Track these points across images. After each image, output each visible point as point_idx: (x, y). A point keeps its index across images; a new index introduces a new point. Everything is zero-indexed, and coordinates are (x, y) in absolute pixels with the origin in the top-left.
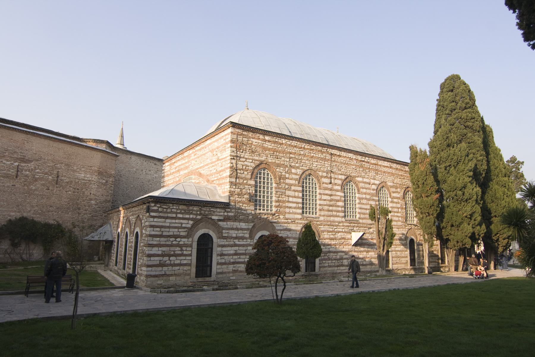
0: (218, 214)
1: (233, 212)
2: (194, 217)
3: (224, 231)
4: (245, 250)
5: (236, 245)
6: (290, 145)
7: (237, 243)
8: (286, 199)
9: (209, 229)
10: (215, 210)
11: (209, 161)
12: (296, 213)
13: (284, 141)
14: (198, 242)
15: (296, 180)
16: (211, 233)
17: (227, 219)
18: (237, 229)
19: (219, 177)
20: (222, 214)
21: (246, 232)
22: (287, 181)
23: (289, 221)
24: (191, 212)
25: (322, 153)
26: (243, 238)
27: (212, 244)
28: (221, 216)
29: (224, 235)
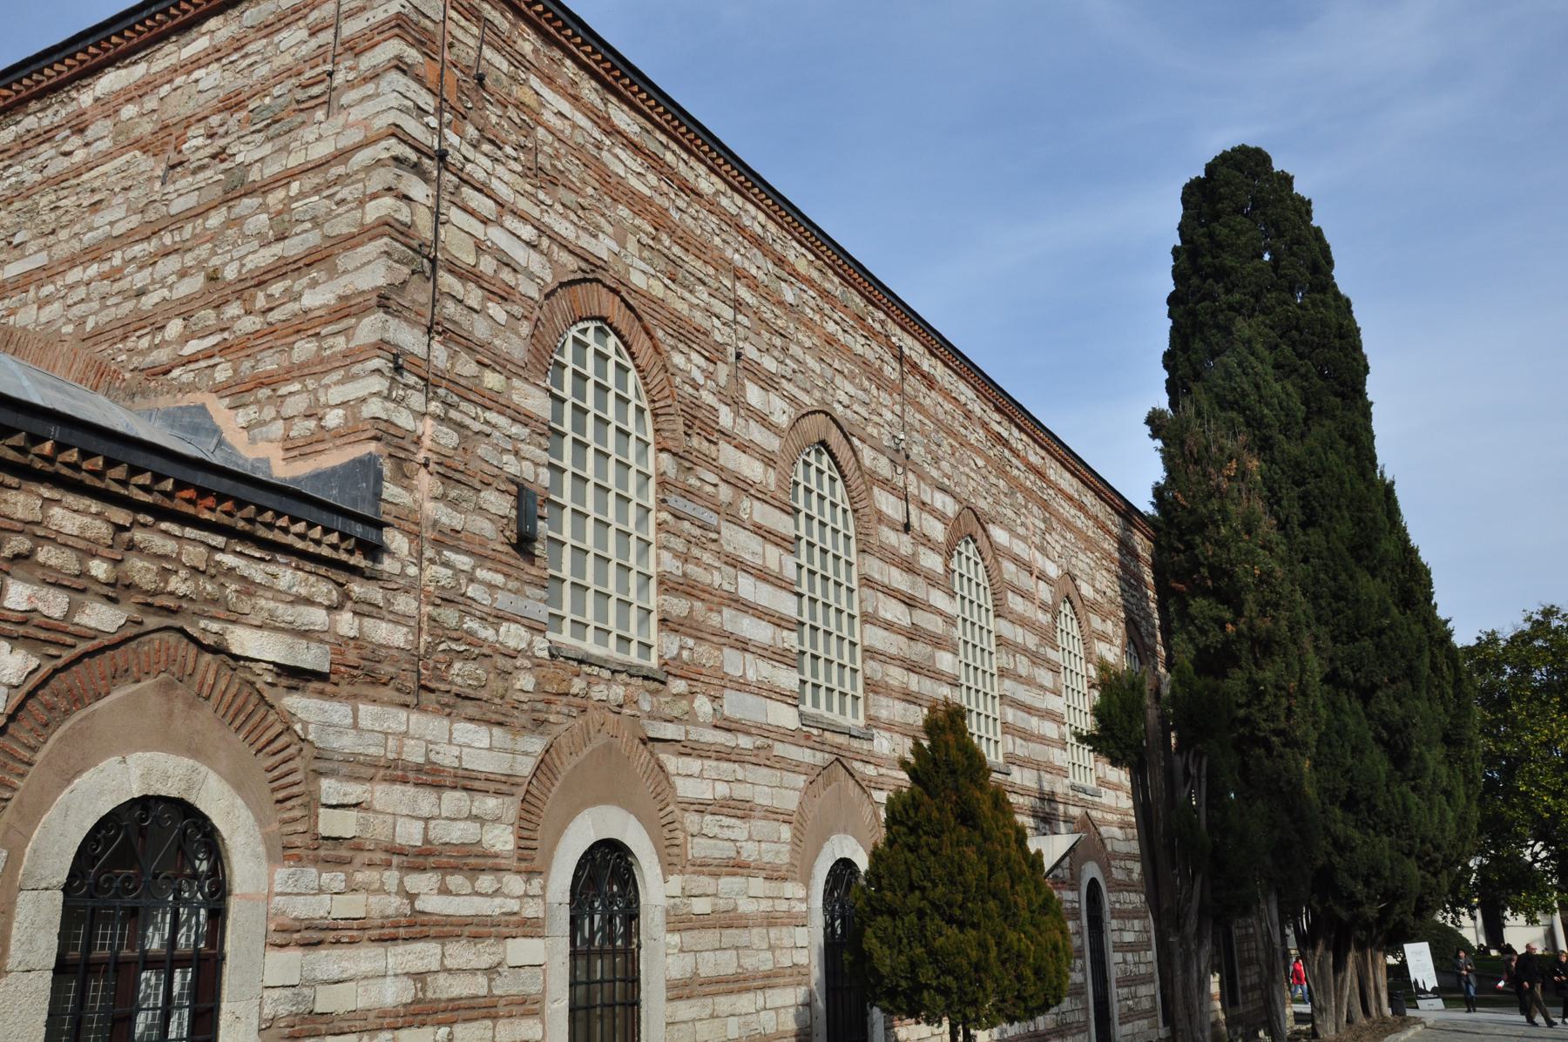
0: (286, 613)
1: (399, 619)
2: (55, 604)
3: (330, 789)
4: (491, 971)
5: (414, 927)
7: (432, 903)
8: (718, 579)
9: (194, 752)
10: (257, 572)
11: (116, 218)
13: (707, 184)
14: (67, 889)
16: (218, 801)
17: (356, 673)
18: (431, 777)
19: (250, 324)
20: (317, 617)
21: (491, 804)
23: (745, 742)
24: (19, 544)
25: (870, 335)
26: (470, 861)
27: (218, 916)
28: (305, 634)
29: (332, 824)
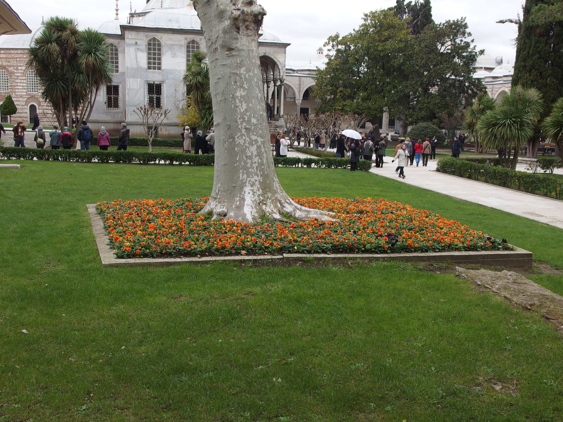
6: (17, 53)
12: (22, 92)
15: (21, 73)
22: (16, 74)
